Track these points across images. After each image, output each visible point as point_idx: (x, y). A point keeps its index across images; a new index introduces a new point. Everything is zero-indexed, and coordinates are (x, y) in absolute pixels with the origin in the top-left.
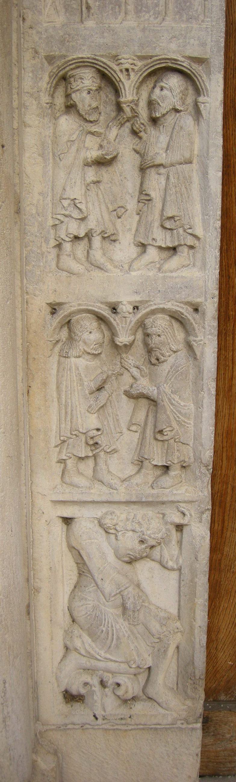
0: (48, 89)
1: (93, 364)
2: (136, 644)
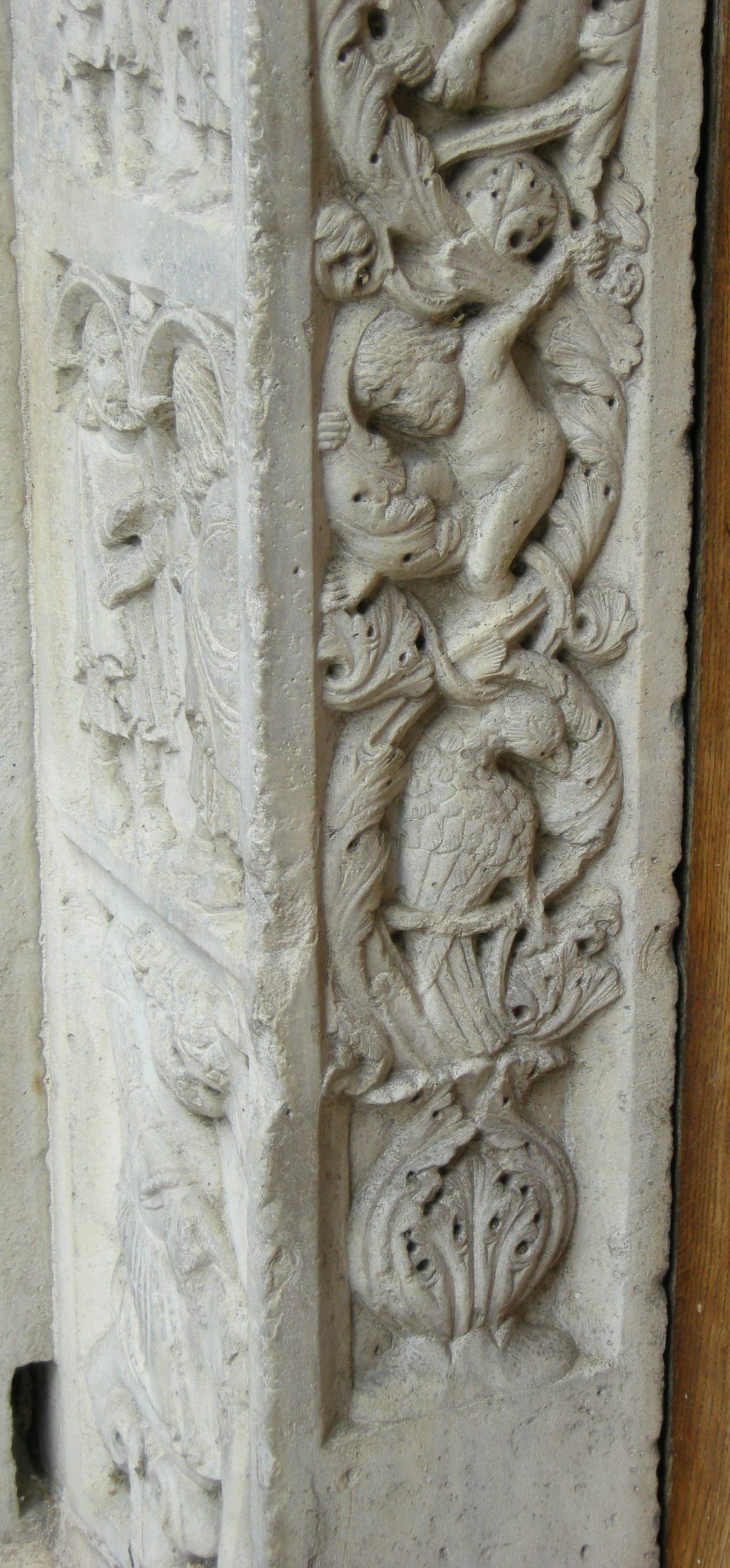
1: (127, 461)
2: (188, 1380)
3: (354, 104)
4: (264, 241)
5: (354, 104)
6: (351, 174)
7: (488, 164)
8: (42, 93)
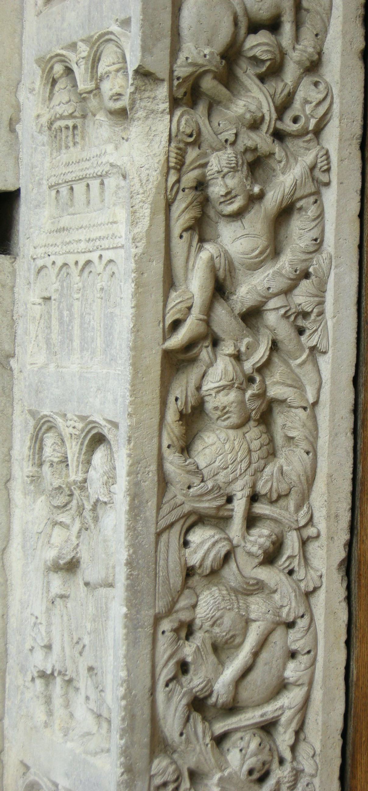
0: (31, 457)
3: (173, 708)
4: (125, 777)
5: (173, 708)
6: (170, 742)
7: (239, 735)
8: (20, 682)
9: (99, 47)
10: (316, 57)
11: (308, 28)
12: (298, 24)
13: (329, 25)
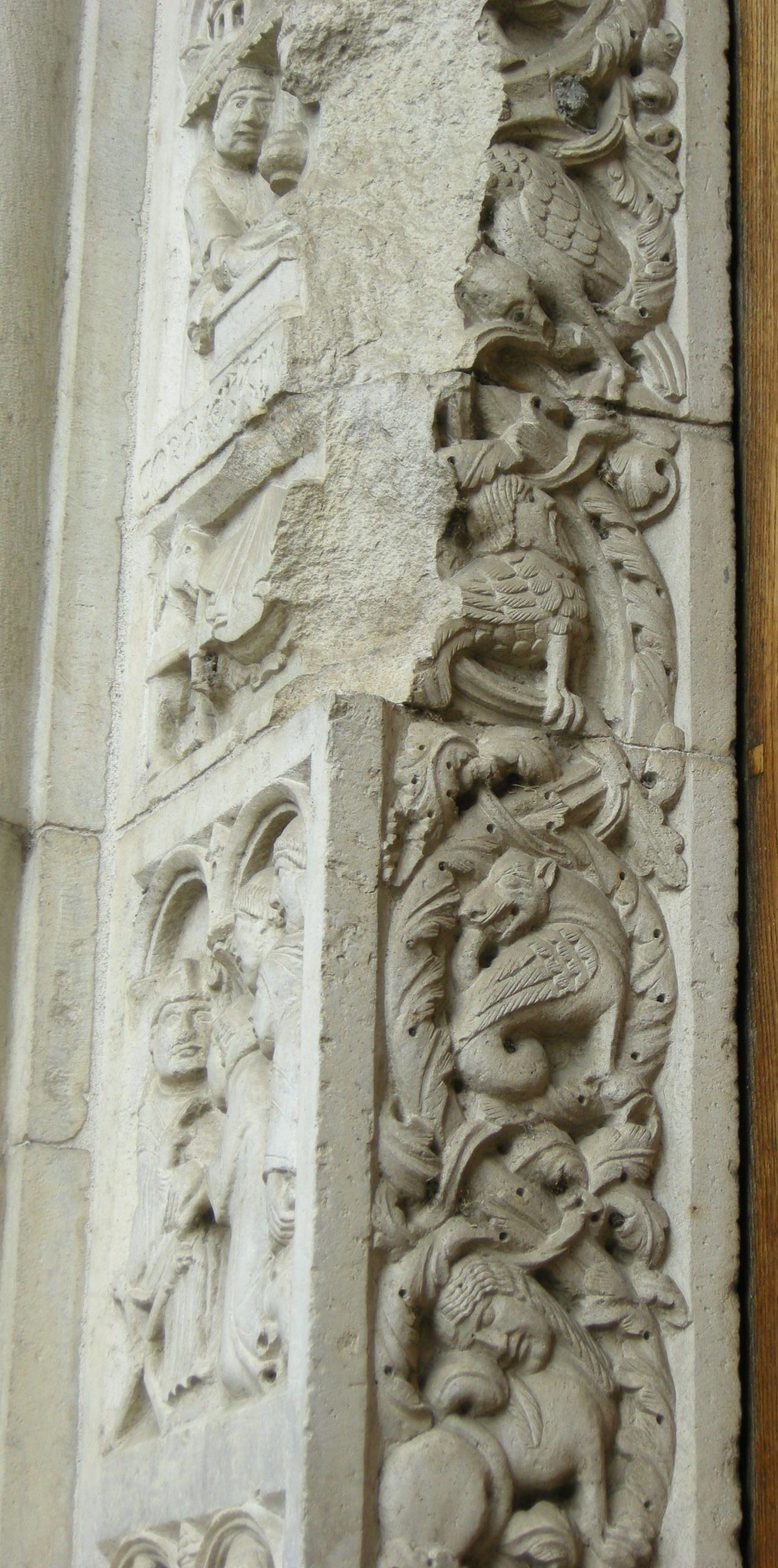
9: (222, 1538)
10: (646, 1549)
11: (630, 1492)
12: (610, 1485)
13: (670, 1483)
